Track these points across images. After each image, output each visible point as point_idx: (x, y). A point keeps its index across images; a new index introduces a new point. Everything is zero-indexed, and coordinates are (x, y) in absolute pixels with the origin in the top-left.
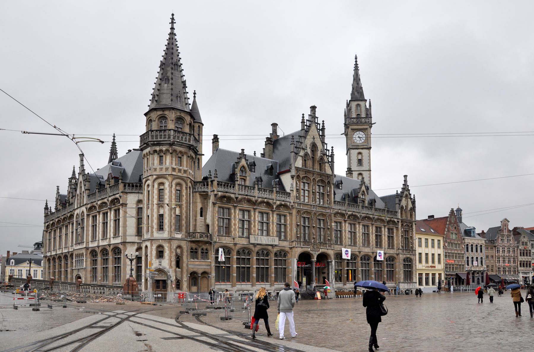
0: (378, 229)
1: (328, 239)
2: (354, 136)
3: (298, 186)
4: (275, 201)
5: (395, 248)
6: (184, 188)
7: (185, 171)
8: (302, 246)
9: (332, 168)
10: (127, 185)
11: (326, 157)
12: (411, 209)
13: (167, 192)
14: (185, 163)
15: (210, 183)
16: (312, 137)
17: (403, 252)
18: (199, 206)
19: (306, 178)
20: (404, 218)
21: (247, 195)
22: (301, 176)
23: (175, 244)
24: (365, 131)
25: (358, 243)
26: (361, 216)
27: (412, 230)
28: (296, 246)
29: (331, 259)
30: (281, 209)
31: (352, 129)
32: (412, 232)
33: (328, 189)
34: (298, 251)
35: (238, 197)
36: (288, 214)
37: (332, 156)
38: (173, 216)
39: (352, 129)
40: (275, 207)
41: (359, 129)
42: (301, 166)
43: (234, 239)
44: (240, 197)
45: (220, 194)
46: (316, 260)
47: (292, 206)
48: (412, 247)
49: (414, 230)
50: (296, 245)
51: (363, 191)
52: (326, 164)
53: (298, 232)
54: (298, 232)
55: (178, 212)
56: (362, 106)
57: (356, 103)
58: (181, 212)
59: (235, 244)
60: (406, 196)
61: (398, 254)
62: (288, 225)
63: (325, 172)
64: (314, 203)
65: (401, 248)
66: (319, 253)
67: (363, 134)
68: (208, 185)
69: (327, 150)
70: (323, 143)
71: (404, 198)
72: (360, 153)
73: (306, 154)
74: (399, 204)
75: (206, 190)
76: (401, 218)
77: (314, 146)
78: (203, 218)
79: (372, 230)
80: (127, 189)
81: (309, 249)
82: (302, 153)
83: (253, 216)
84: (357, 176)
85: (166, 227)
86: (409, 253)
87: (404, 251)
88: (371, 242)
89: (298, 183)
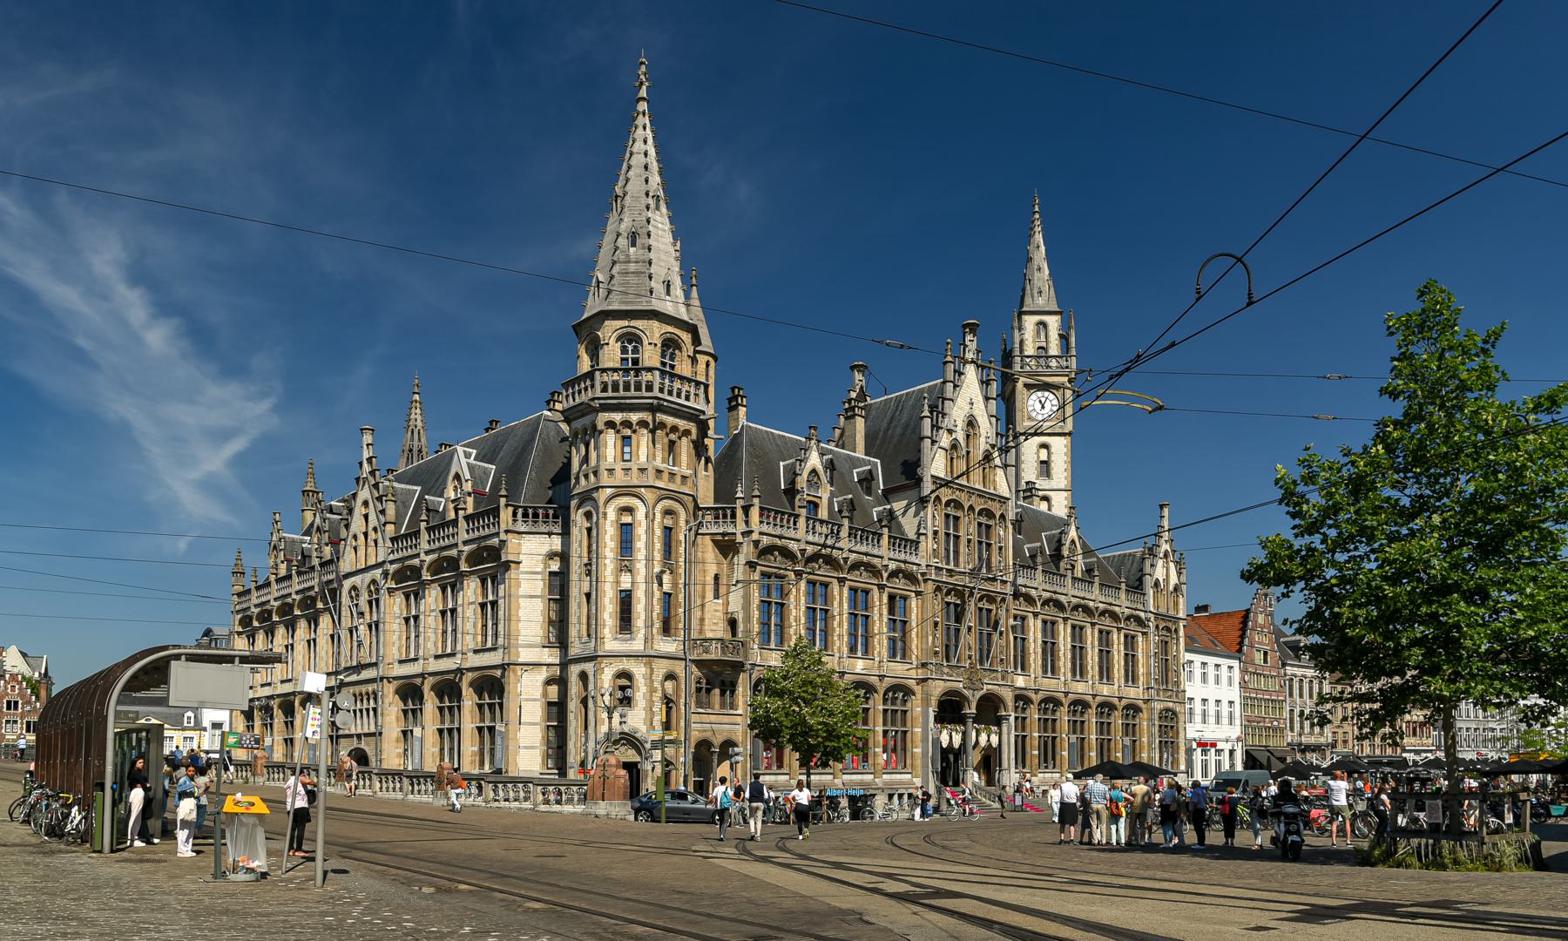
0: (1105, 636)
1: (1002, 660)
2: (1031, 402)
4: (885, 563)
5: (1141, 683)
10: (520, 511)
13: (640, 531)
14: (684, 458)
15: (739, 513)
17: (1158, 695)
18: (712, 569)
20: (1162, 610)
23: (661, 668)
25: (1062, 670)
26: (1069, 602)
27: (1178, 639)
32: (1177, 644)
33: (1002, 533)
34: (938, 689)
35: (805, 550)
38: (657, 594)
40: (885, 575)
42: (942, 475)
46: (975, 711)
47: (923, 574)
48: (1177, 683)
49: (1182, 640)
51: (1073, 542)
55: (666, 587)
56: (1050, 328)
58: (675, 584)
66: (981, 693)
67: (1051, 397)
68: (734, 516)
72: (1044, 446)
73: (954, 446)
75: (730, 530)
77: (971, 423)
78: (720, 601)
79: (1091, 638)
80: (520, 523)
82: (945, 440)
83: (838, 597)
85: (639, 622)
86: (1170, 697)
87: (1161, 693)
88: (1089, 668)
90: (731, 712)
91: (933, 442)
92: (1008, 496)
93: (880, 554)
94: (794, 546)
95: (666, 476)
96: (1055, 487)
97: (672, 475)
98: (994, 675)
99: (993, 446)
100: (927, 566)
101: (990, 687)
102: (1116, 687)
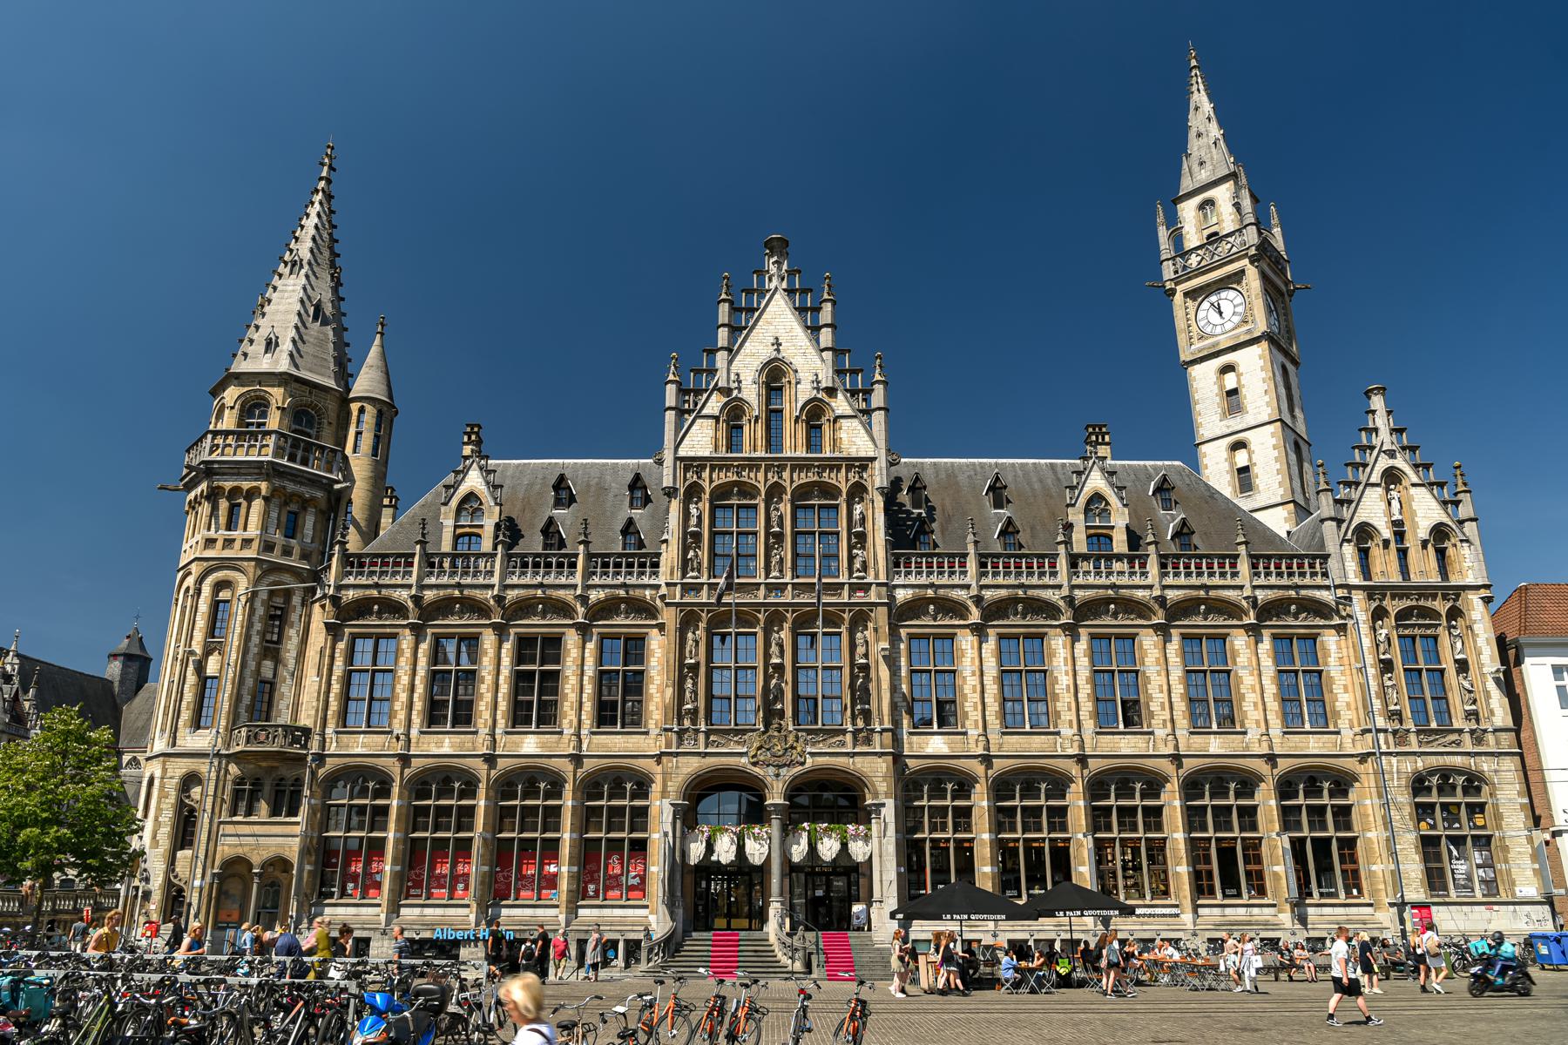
2: (1201, 314)
3: (694, 521)
5: (1343, 724)
7: (247, 542)
16: (772, 340)
24: (1239, 282)
28: (673, 750)
29: (876, 795)
31: (1186, 294)
43: (398, 738)
47: (663, 597)
50: (668, 745)
51: (1097, 497)
65: (1381, 722)
66: (797, 770)
67: (1231, 294)
72: (1228, 368)
74: (1339, 522)
82: (714, 405)
84: (1224, 454)
89: (694, 511)
91: (681, 412)
92: (871, 454)
94: (403, 595)
95: (219, 544)
96: (1253, 423)
99: (831, 391)
100: (668, 585)
101: (821, 760)
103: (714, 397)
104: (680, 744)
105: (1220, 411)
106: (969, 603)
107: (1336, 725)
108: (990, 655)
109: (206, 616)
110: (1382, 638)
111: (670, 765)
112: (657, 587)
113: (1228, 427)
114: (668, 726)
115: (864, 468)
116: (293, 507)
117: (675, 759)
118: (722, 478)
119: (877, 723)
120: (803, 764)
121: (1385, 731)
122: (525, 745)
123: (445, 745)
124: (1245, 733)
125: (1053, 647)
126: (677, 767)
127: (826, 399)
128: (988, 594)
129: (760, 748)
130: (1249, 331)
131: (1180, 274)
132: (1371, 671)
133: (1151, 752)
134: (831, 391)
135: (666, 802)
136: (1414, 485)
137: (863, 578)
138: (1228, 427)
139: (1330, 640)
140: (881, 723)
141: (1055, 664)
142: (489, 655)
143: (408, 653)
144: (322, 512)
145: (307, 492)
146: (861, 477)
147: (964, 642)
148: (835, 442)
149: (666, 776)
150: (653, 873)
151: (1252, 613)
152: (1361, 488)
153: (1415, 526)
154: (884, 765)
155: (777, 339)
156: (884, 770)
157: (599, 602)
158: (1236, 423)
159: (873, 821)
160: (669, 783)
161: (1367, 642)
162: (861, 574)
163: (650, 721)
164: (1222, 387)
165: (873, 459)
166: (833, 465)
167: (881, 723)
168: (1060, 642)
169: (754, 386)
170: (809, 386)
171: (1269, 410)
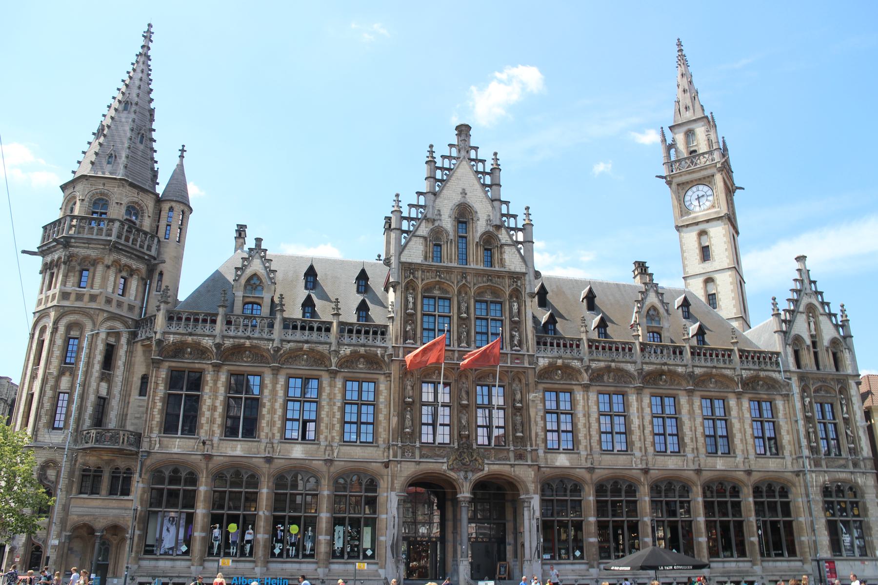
1: (517, 437)
2: (687, 198)
3: (411, 305)
5: (787, 453)
6: (88, 333)
7: (93, 298)
8: (417, 459)
9: (527, 259)
11: (503, 231)
12: (834, 342)
18: (140, 369)
19: (437, 286)
21: (249, 338)
22: (420, 285)
24: (710, 182)
25: (638, 444)
28: (399, 459)
29: (527, 492)
30: (361, 366)
31: (678, 185)
36: (382, 378)
37: (527, 228)
39: (678, 185)
40: (334, 360)
41: (696, 180)
43: (204, 443)
44: (228, 343)
45: (172, 338)
50: (395, 456)
52: (507, 249)
53: (408, 423)
54: (408, 423)
57: (685, 128)
59: (208, 457)
60: (811, 308)
61: (797, 474)
62: (382, 406)
63: (503, 265)
64: (464, 344)
65: (806, 452)
66: (480, 474)
67: (706, 188)
69: (509, 216)
70: (496, 200)
71: (804, 316)
74: (785, 333)
76: (799, 366)
78: (146, 398)
81: (445, 467)
82: (424, 230)
88: (687, 440)
89: (411, 299)
90: (122, 497)
92: (524, 270)
93: (328, 341)
94: (207, 342)
95: (73, 297)
97: (79, 297)
98: (505, 454)
99: (498, 227)
100: (393, 347)
101: (495, 468)
102: (740, 459)
103: (423, 224)
104: (403, 455)
105: (698, 258)
106: (583, 371)
107: (783, 454)
108: (593, 404)
109: (61, 348)
110: (807, 403)
111: (396, 469)
112: (386, 348)
113: (703, 268)
114: (394, 443)
115: (519, 278)
116: (124, 274)
117: (399, 466)
118: (431, 279)
119: (529, 445)
120: (483, 470)
121: (809, 458)
122: (294, 452)
123: (238, 449)
124: (736, 457)
125: (630, 401)
126: (401, 471)
127: (496, 233)
128: (594, 365)
129: (454, 460)
130: (716, 212)
131: (674, 172)
132: (801, 423)
133: (685, 468)
134: (498, 227)
135: (393, 494)
136: (821, 314)
137: (519, 351)
138: (703, 268)
139: (780, 404)
140: (531, 446)
141: (631, 411)
142: (269, 388)
143: (211, 383)
144: (143, 279)
145: (134, 264)
146: (517, 285)
147: (578, 396)
148: (502, 262)
149: (394, 477)
150: (382, 541)
151: (740, 385)
152: (795, 314)
153: (822, 339)
154: (533, 473)
155: (464, 189)
156: (533, 476)
157: (346, 356)
158: (708, 267)
159: (525, 509)
160: (395, 481)
161: (798, 405)
162: (518, 348)
163: (380, 439)
164: (700, 244)
165: (524, 274)
166: (499, 275)
167: (531, 446)
168: (634, 398)
169: (450, 219)
170: (484, 223)
171: (728, 261)
